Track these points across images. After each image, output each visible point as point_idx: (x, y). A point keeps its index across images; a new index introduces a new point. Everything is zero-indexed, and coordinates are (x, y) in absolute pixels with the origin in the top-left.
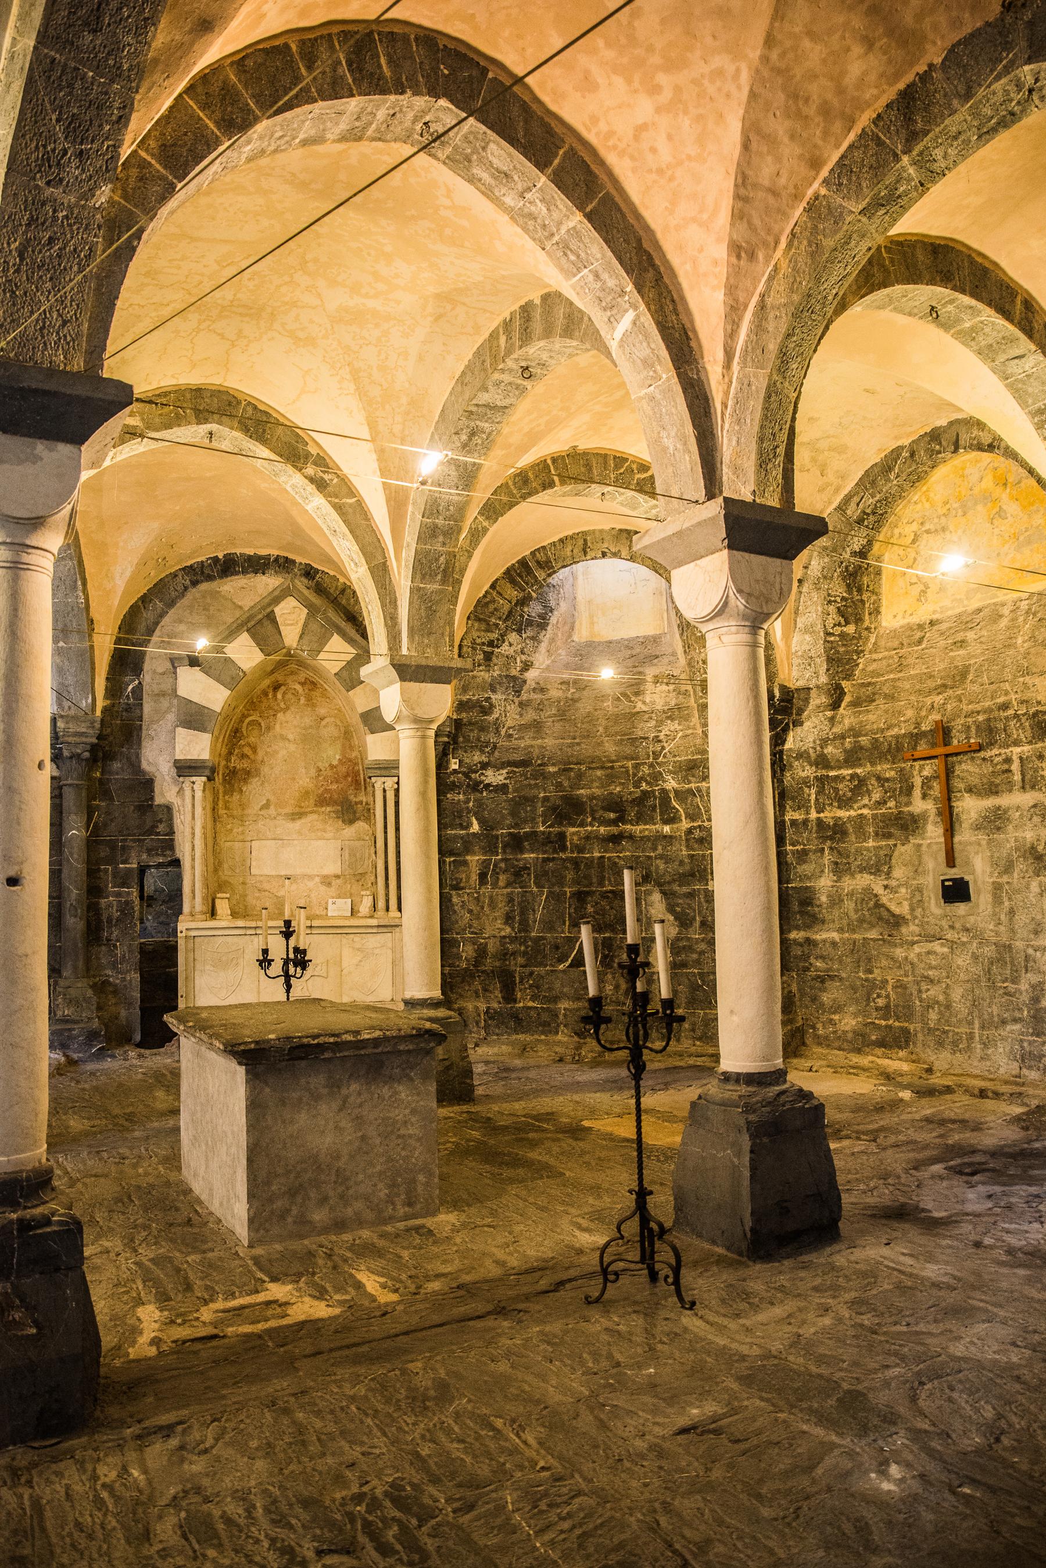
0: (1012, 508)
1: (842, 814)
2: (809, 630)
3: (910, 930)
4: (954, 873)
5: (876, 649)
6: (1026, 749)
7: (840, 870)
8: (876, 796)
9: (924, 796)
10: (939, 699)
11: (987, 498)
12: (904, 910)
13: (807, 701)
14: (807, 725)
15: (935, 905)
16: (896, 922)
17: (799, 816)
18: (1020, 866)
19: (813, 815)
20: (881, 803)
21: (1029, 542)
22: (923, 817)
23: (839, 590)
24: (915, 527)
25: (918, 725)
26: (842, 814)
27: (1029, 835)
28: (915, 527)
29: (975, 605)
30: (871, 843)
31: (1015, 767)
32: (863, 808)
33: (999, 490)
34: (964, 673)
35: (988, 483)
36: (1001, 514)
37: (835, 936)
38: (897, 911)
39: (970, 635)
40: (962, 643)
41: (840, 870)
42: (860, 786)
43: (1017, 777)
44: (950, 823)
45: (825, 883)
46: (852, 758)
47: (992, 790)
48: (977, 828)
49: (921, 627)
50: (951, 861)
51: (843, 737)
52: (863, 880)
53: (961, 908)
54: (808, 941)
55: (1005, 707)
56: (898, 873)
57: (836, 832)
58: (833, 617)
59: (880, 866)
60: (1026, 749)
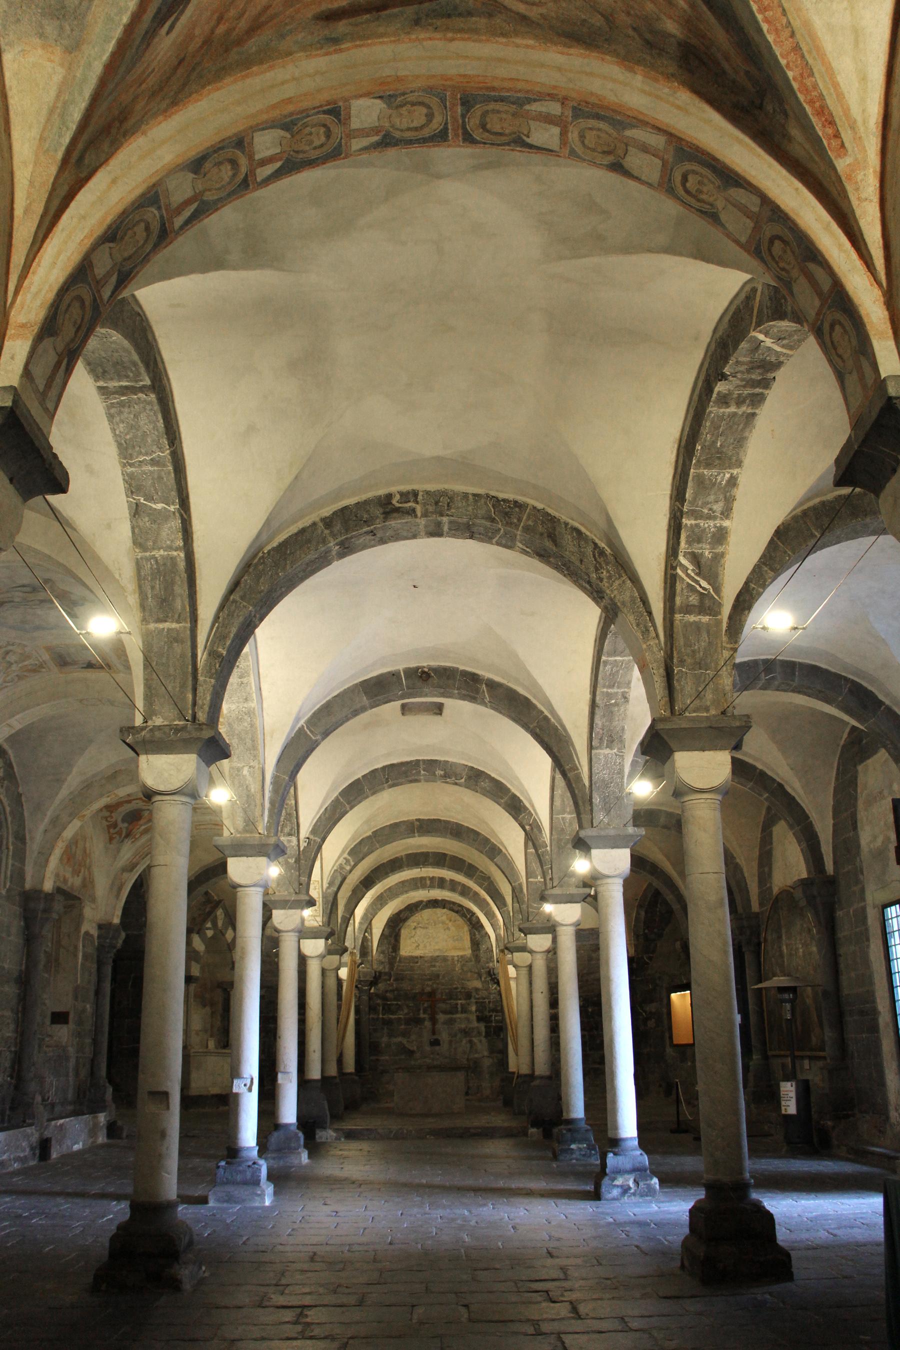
0: (453, 928)
1: (391, 1016)
2: (383, 952)
3: (418, 1055)
4: (435, 1037)
5: (400, 961)
6: (463, 1002)
7: (390, 1035)
8: (406, 1011)
9: (424, 1013)
10: (430, 983)
11: (443, 923)
12: (415, 1048)
13: (380, 976)
14: (380, 985)
15: (428, 1048)
16: (412, 1053)
17: (375, 1016)
18: (459, 1036)
19: (381, 1016)
20: (406, 1014)
21: (457, 940)
22: (424, 1019)
23: (393, 941)
24: (415, 924)
25: (423, 990)
26: (391, 1016)
27: (463, 1026)
28: (415, 924)
29: (437, 954)
30: (403, 1027)
31: (459, 1006)
32: (401, 1015)
33: (447, 922)
34: (438, 976)
35: (444, 918)
36: (448, 929)
37: (387, 1058)
38: (411, 1049)
39: (437, 964)
40: (434, 966)
41: (390, 1035)
42: (399, 1008)
43: (459, 1009)
44: (434, 1021)
45: (385, 1039)
46: (395, 999)
47: (451, 1013)
48: (444, 1023)
49: (417, 957)
50: (434, 1032)
51: (393, 991)
52: (399, 1039)
53: (437, 1048)
54: (377, 1060)
55: (456, 988)
56: (413, 1037)
57: (389, 1023)
58: (390, 950)
59: (405, 1034)
60: (463, 1002)
